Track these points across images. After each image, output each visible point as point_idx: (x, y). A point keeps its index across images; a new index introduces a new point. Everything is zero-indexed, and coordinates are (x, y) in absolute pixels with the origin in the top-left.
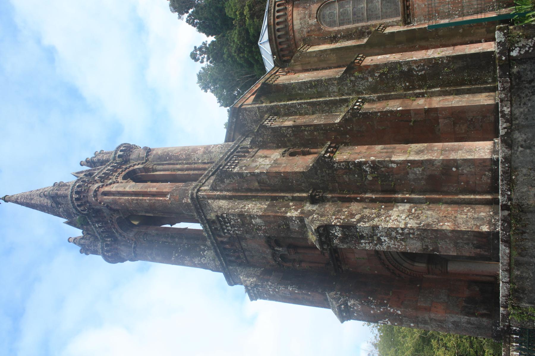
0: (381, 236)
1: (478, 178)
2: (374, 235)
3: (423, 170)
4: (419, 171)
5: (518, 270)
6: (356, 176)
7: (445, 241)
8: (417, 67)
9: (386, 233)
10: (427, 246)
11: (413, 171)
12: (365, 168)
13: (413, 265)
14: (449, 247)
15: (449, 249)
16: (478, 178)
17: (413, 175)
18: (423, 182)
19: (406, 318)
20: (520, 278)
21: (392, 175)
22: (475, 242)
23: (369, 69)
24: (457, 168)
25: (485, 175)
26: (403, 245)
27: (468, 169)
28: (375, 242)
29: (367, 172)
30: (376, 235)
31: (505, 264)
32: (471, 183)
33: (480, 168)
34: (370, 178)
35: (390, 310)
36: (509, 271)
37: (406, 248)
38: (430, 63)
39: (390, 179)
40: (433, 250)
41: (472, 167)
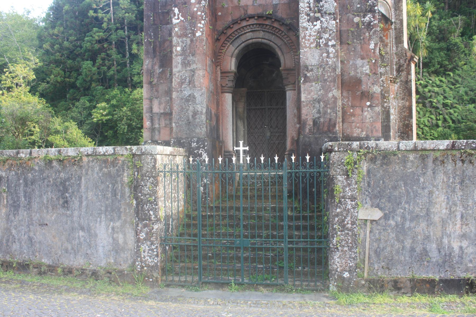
0: (321, 21)
1: (358, 125)
2: (321, 14)
3: (367, 74)
4: (365, 70)
5: (415, 158)
6: (359, 6)
7: (320, 90)
8: (382, 81)
9: (327, 28)
10: (312, 70)
11: (365, 64)
12: (369, 16)
13: (232, 57)
14: (312, 94)
15: (309, 93)
16: (358, 125)
17: (361, 64)
18: (352, 73)
19: (189, 42)
20: (404, 160)
21: (361, 43)
22: (322, 120)
23: (384, 38)
24: (370, 106)
25: (362, 131)
26: (310, 44)
27: (368, 116)
28: (312, 14)
29: (364, 18)
30: (322, 16)
31: (425, 145)
32: (353, 118)
33: (370, 127)
34: (356, 20)
35: (201, 23)
36: (415, 150)
37: (306, 47)
38: (385, 92)
39: (355, 41)
40: (305, 76)
41: (371, 119)
